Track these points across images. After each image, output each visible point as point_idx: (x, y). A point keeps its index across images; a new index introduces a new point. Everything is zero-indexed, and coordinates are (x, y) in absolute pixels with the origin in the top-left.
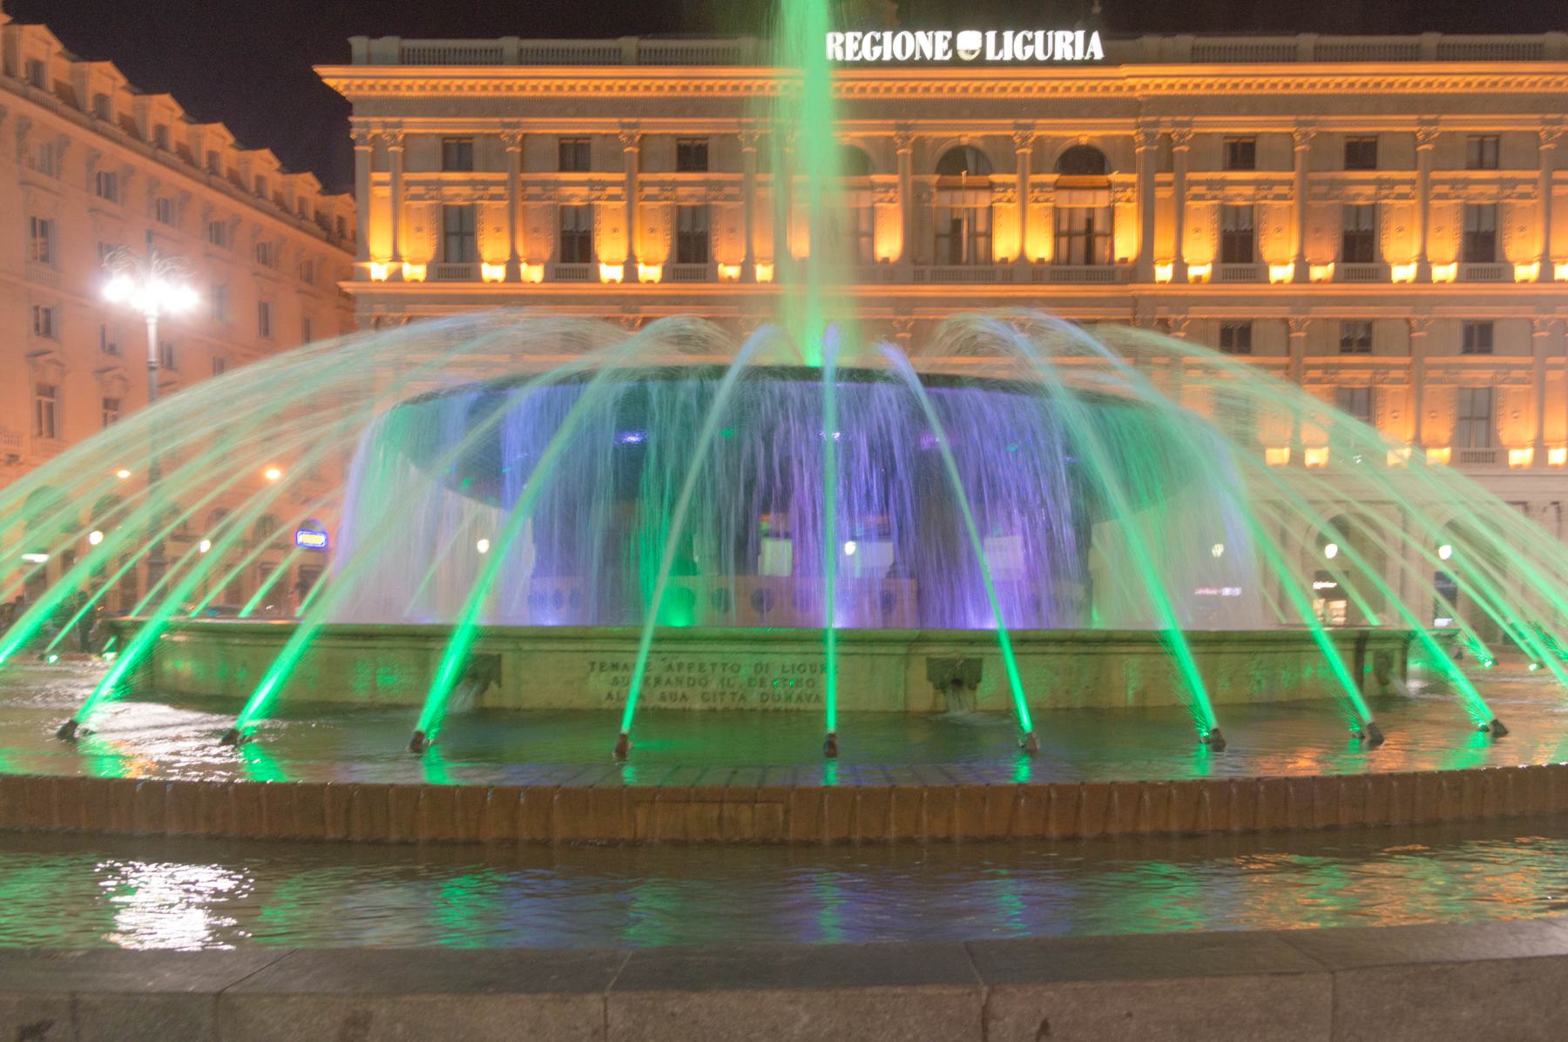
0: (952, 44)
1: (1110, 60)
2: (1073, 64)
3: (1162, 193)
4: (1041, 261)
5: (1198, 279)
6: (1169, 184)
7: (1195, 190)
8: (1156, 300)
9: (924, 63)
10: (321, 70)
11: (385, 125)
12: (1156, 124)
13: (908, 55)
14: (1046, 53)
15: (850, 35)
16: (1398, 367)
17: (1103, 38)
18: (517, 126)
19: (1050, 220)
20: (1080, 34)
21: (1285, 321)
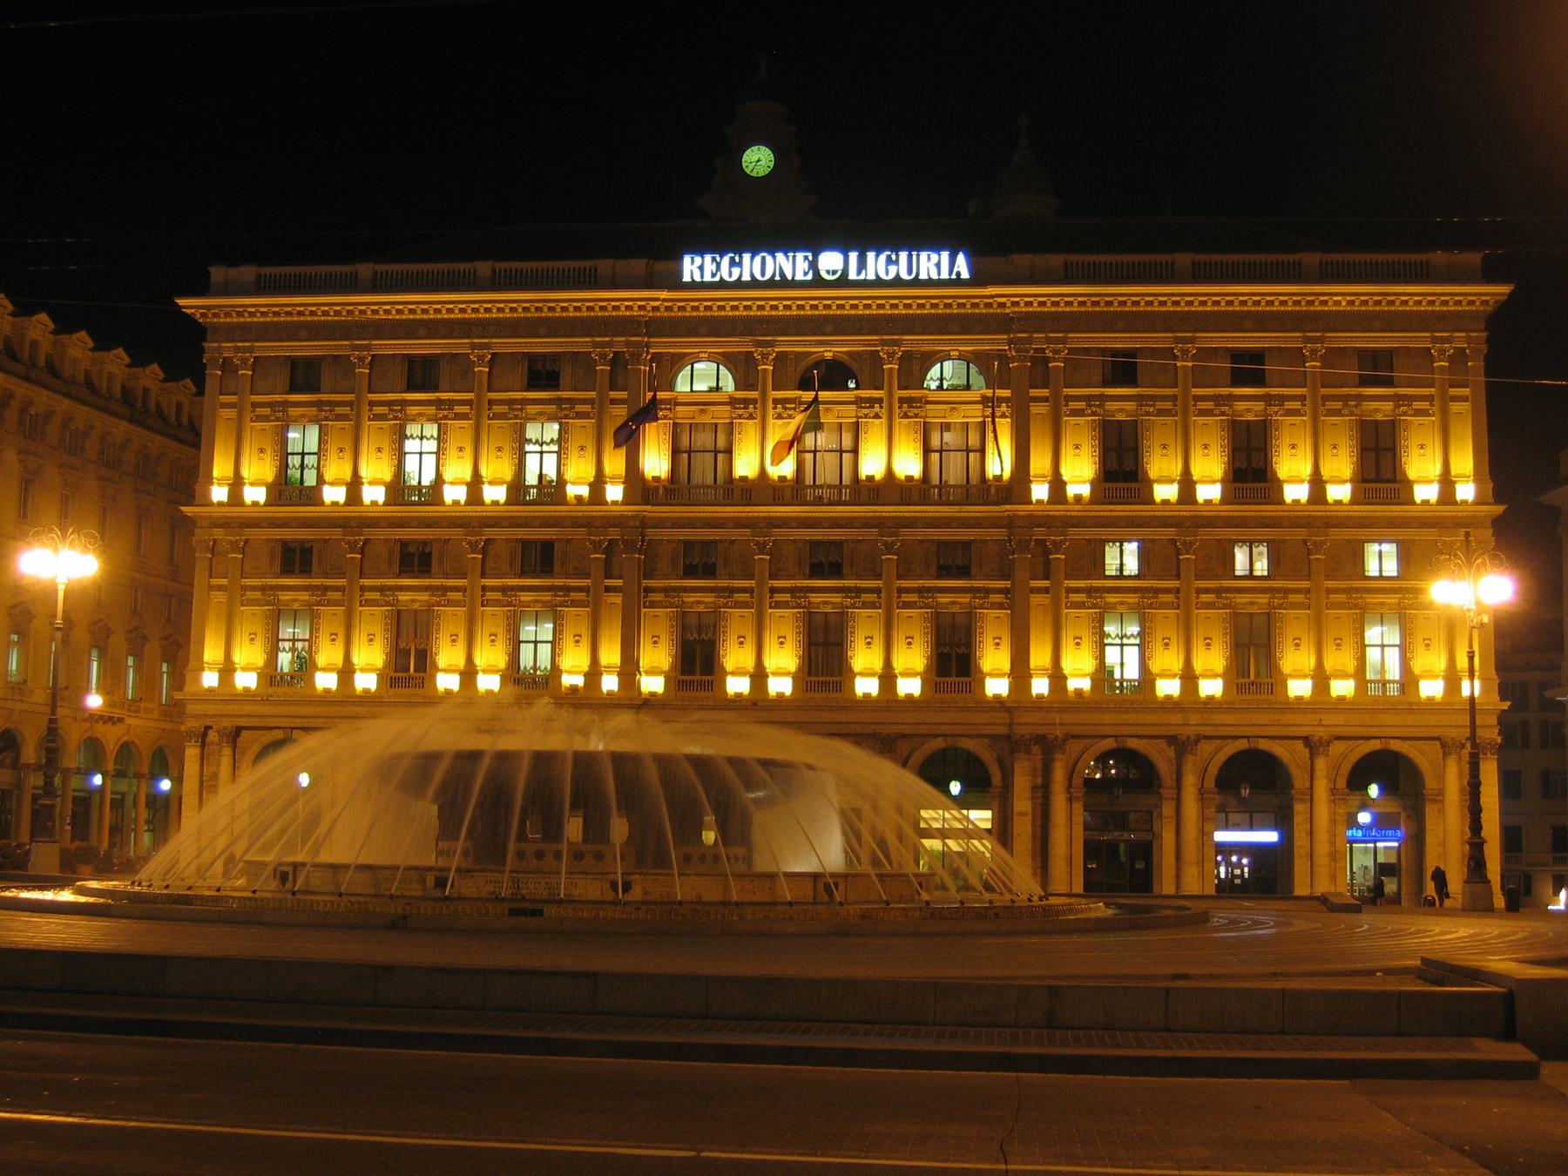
0: (814, 265)
1: (977, 279)
2: (940, 283)
3: (1036, 409)
4: (909, 478)
5: (1078, 498)
6: (1046, 399)
7: (1073, 405)
8: (1035, 521)
9: (785, 283)
10: (181, 302)
11: (237, 350)
12: (1030, 341)
13: (768, 276)
14: (910, 272)
15: (708, 258)
16: (1298, 591)
17: (967, 257)
18: (368, 348)
19: (920, 436)
20: (945, 255)
21: (1173, 542)
